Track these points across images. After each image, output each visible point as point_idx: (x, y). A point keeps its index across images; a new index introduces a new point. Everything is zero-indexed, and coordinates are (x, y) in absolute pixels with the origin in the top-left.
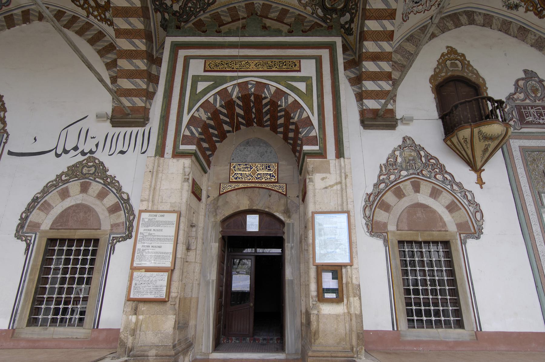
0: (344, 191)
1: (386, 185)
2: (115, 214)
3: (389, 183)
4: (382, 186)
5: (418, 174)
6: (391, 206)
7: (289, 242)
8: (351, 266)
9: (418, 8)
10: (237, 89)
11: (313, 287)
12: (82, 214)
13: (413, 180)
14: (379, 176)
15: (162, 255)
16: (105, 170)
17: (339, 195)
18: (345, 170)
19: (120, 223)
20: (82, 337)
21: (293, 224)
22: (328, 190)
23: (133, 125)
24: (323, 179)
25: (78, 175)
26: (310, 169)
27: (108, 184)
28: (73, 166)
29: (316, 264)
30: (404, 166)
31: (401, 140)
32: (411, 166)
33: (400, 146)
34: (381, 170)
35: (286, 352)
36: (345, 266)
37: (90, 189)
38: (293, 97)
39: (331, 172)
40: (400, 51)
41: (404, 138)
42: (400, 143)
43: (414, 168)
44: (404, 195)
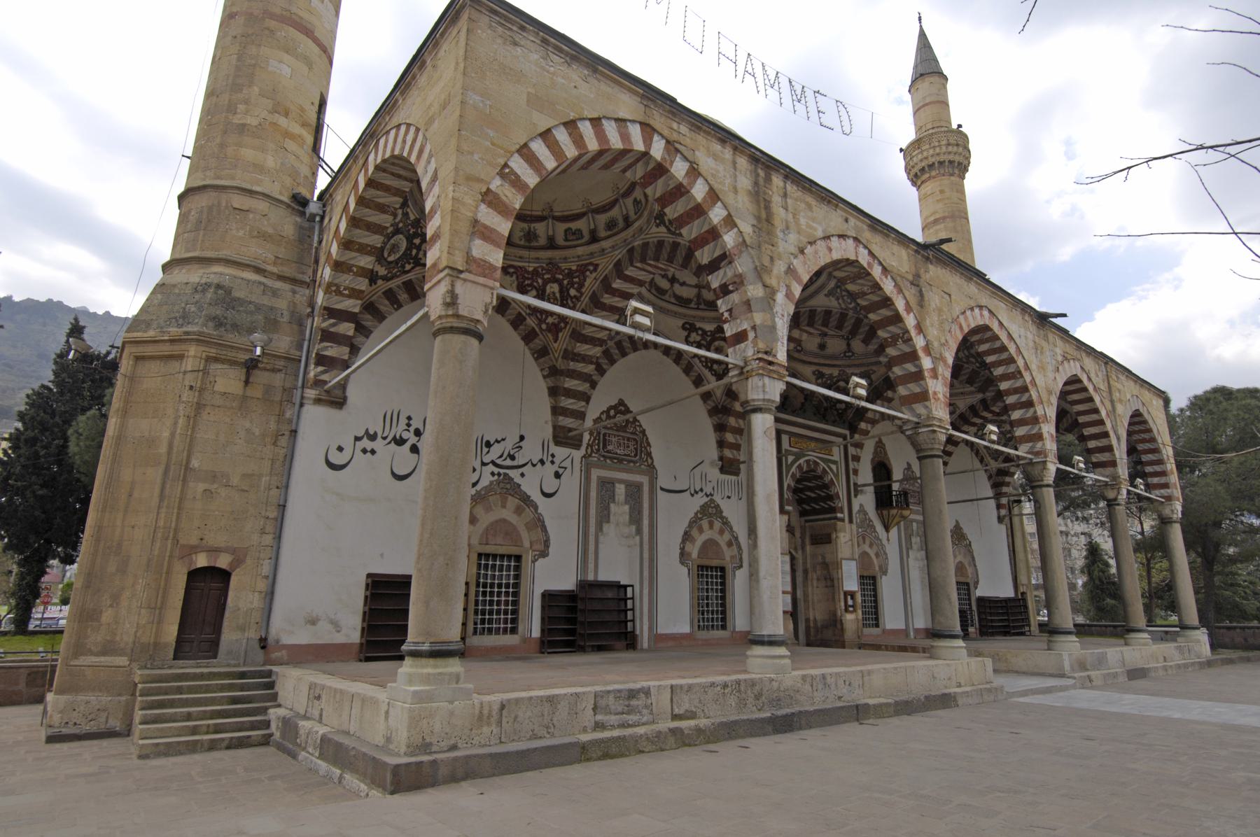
11: (842, 604)
16: (721, 512)
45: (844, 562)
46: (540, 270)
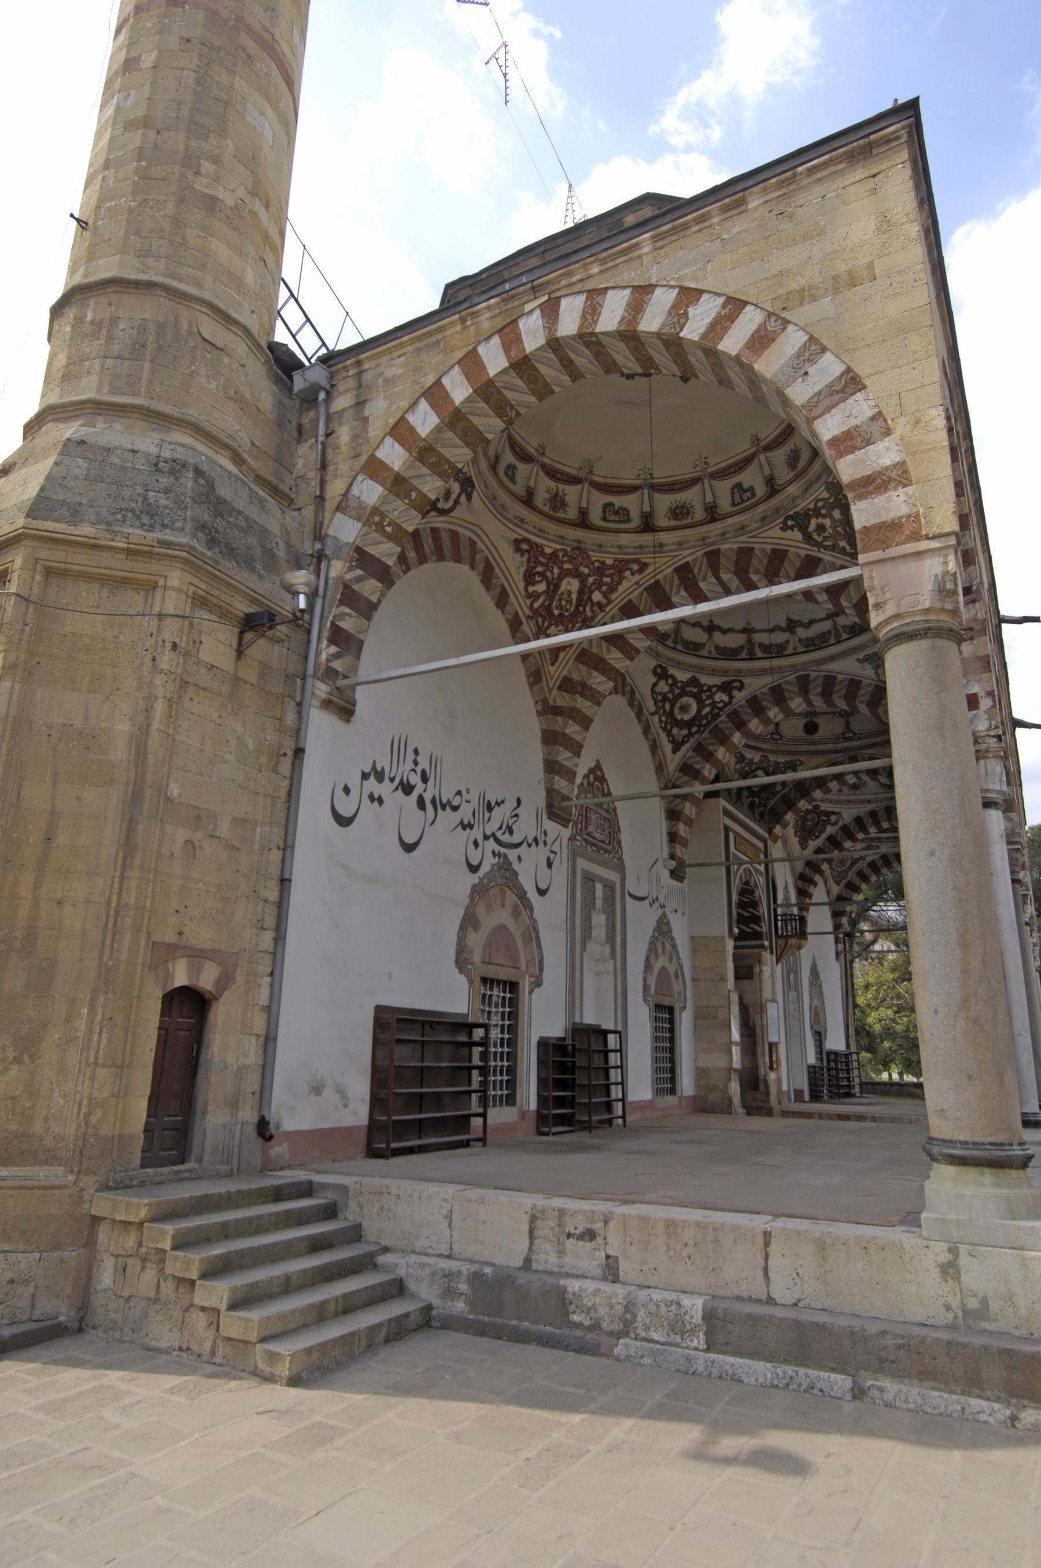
45: (768, 1004)
46: (561, 554)
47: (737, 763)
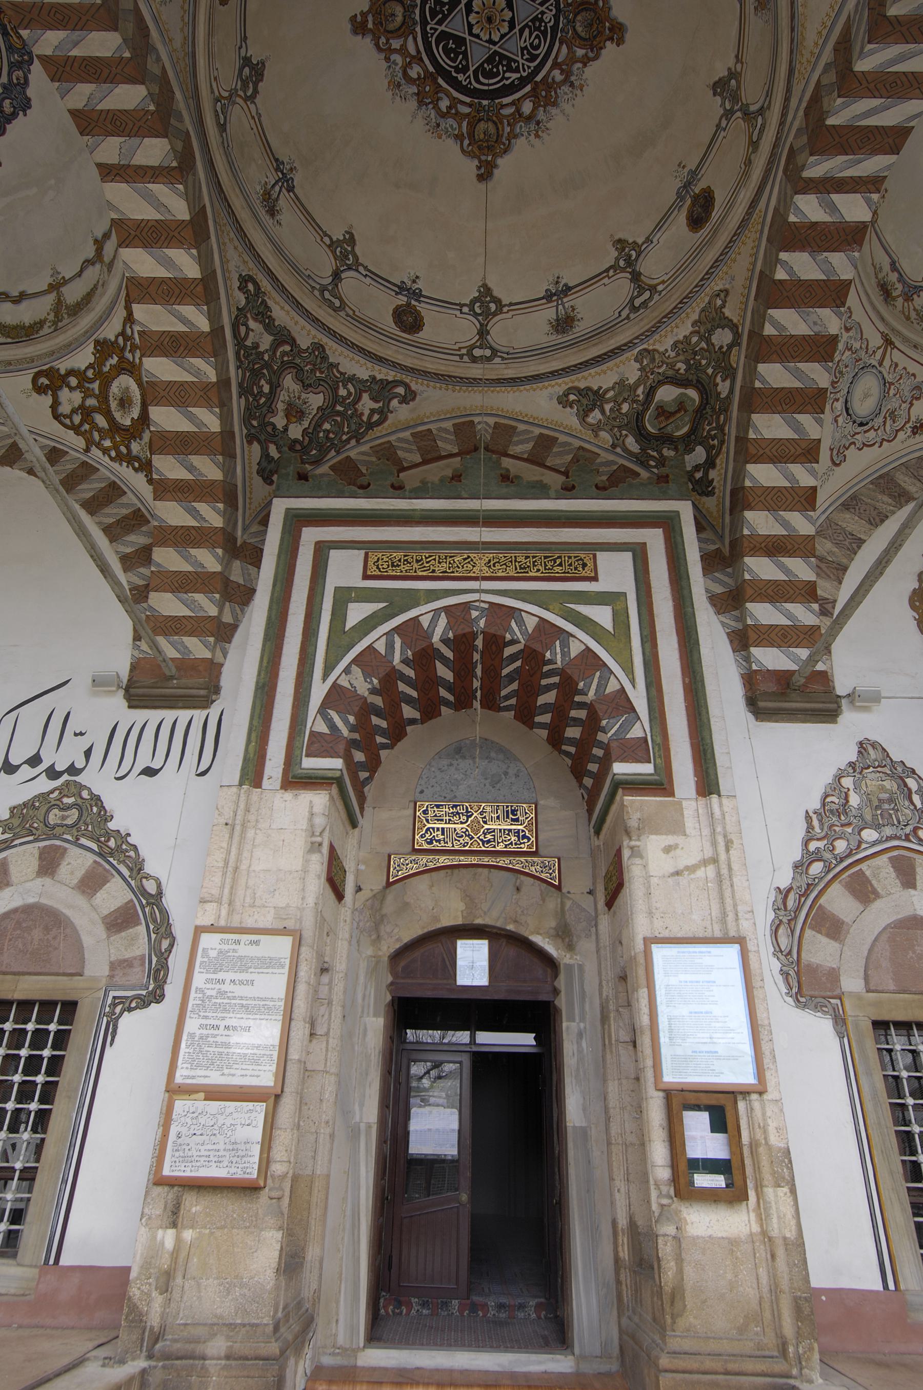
0: (726, 884)
1: (825, 866)
2: (123, 934)
3: (834, 862)
4: (817, 868)
5: (907, 839)
6: (843, 922)
7: (571, 1019)
8: (761, 1093)
9: (867, 435)
10: (443, 621)
11: (659, 1153)
12: (37, 934)
13: (895, 853)
14: (806, 843)
15: (252, 1052)
16: (105, 817)
17: (714, 894)
18: (724, 828)
19: (135, 958)
20: (12, 1291)
21: (581, 967)
22: (683, 880)
23: (180, 704)
24: (668, 850)
25: (36, 829)
26: (633, 823)
27: (110, 853)
28: (25, 805)
29: (662, 1086)
30: (868, 817)
31: (855, 749)
32: (886, 816)
33: (852, 765)
34: (810, 827)
35: (577, 1350)
36: (744, 1092)
37: (61, 866)
38: (581, 640)
39: (688, 832)
40: (830, 532)
41: (861, 743)
42: (852, 755)
43: (896, 823)
44: (877, 895)
45: (660, 953)
47: (583, 415)
